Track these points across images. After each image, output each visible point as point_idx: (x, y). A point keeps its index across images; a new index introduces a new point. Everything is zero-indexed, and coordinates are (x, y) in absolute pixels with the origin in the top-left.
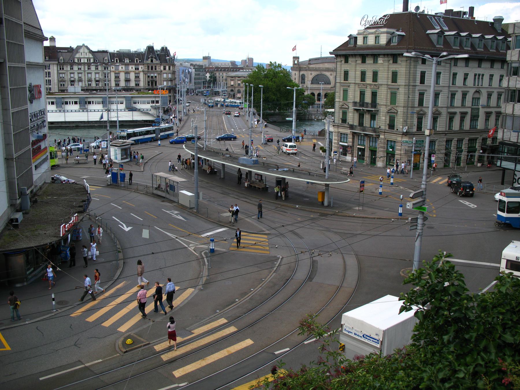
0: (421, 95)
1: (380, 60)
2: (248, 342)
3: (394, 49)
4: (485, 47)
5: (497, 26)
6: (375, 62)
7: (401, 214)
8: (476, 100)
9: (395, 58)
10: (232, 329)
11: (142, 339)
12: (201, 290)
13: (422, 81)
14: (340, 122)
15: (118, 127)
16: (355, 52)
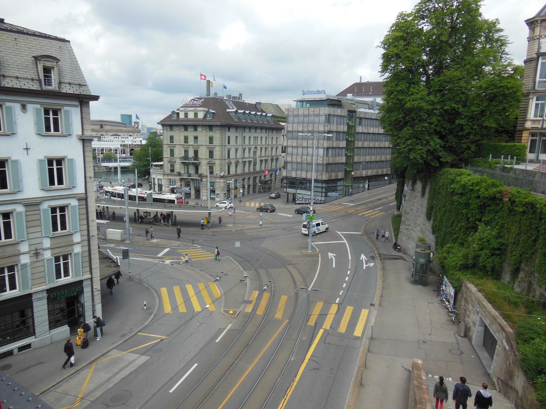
0: (229, 151)
1: (199, 129)
3: (210, 121)
4: (239, 118)
5: (258, 106)
6: (196, 130)
7: (261, 225)
8: (255, 152)
9: (211, 127)
13: (229, 143)
14: (169, 171)
16: (180, 123)
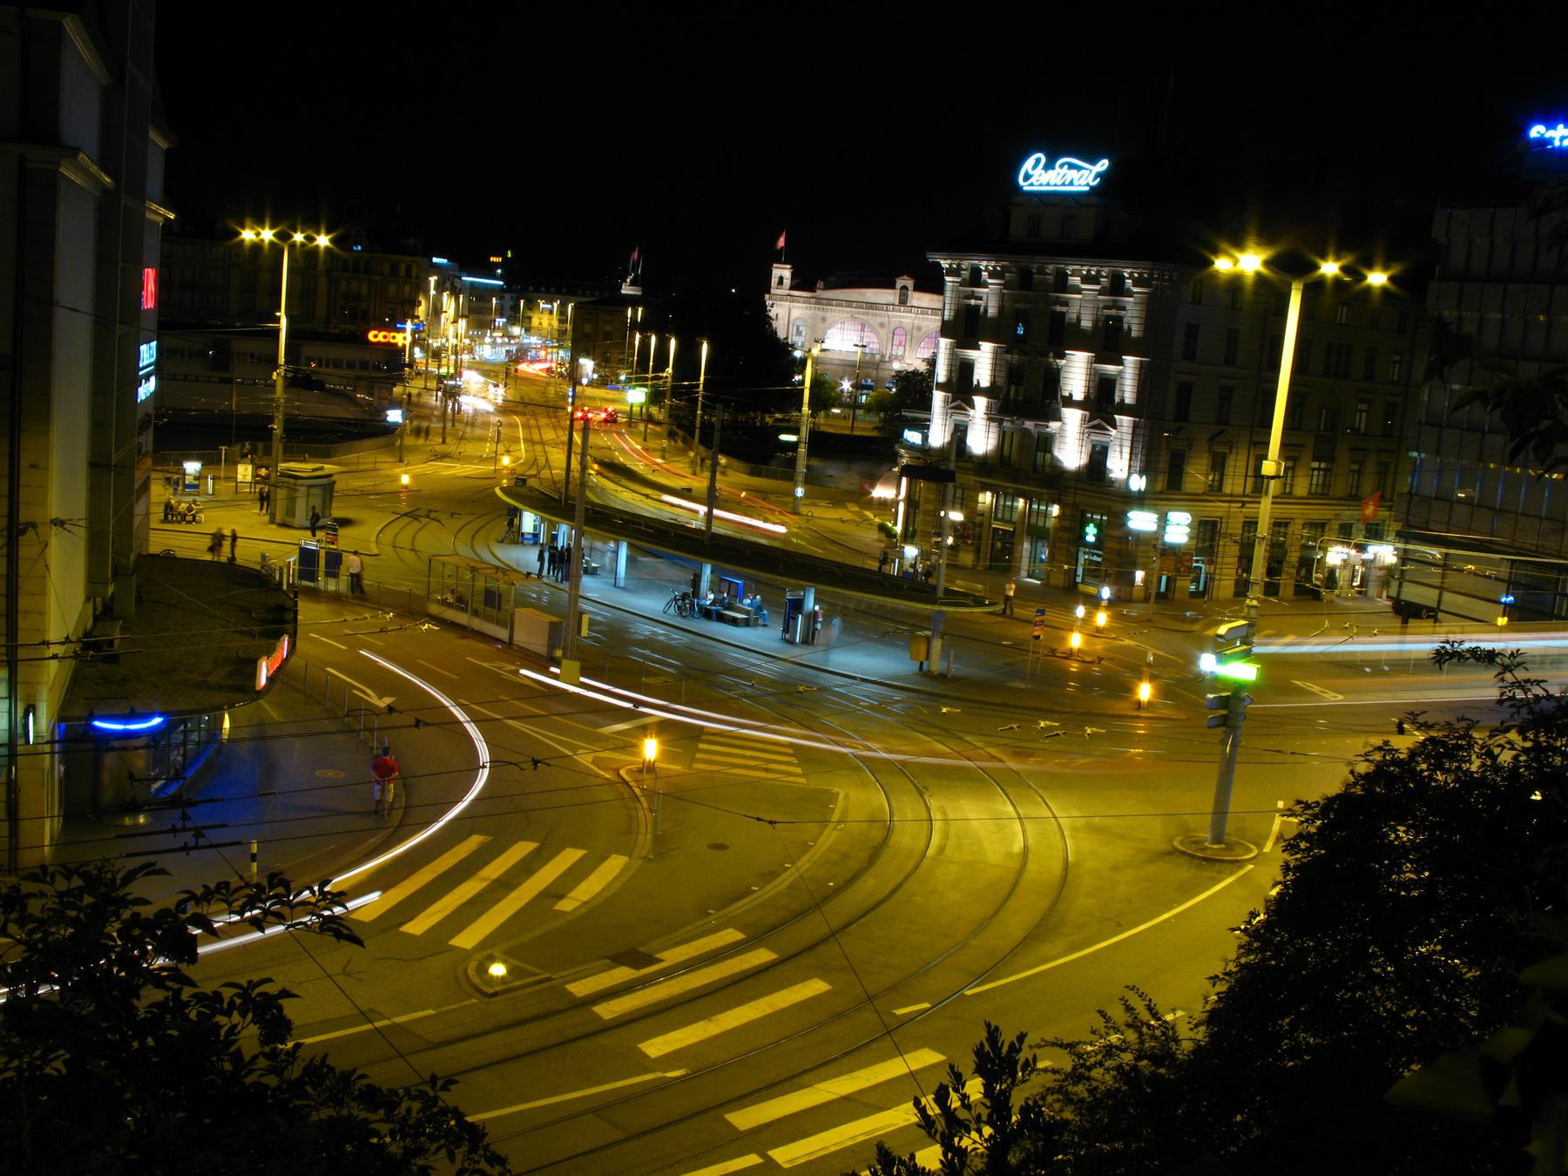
2: (816, 987)
10: (762, 956)
11: (530, 968)
12: (645, 858)
13: (1189, 355)
15: (277, 427)
